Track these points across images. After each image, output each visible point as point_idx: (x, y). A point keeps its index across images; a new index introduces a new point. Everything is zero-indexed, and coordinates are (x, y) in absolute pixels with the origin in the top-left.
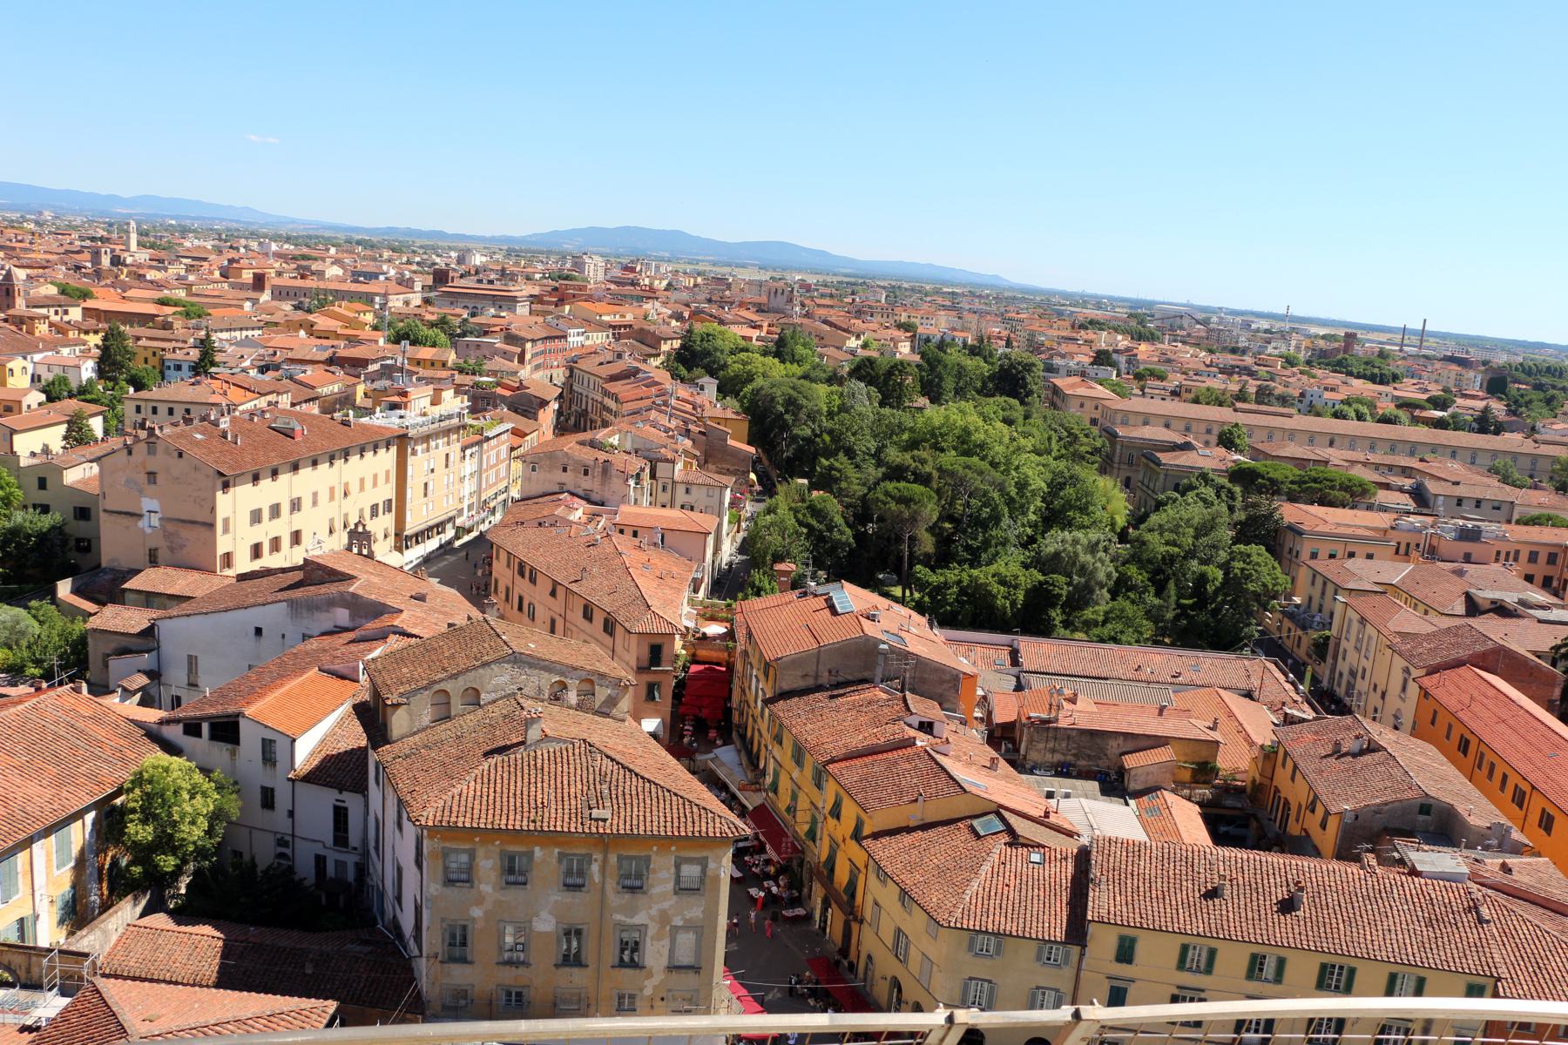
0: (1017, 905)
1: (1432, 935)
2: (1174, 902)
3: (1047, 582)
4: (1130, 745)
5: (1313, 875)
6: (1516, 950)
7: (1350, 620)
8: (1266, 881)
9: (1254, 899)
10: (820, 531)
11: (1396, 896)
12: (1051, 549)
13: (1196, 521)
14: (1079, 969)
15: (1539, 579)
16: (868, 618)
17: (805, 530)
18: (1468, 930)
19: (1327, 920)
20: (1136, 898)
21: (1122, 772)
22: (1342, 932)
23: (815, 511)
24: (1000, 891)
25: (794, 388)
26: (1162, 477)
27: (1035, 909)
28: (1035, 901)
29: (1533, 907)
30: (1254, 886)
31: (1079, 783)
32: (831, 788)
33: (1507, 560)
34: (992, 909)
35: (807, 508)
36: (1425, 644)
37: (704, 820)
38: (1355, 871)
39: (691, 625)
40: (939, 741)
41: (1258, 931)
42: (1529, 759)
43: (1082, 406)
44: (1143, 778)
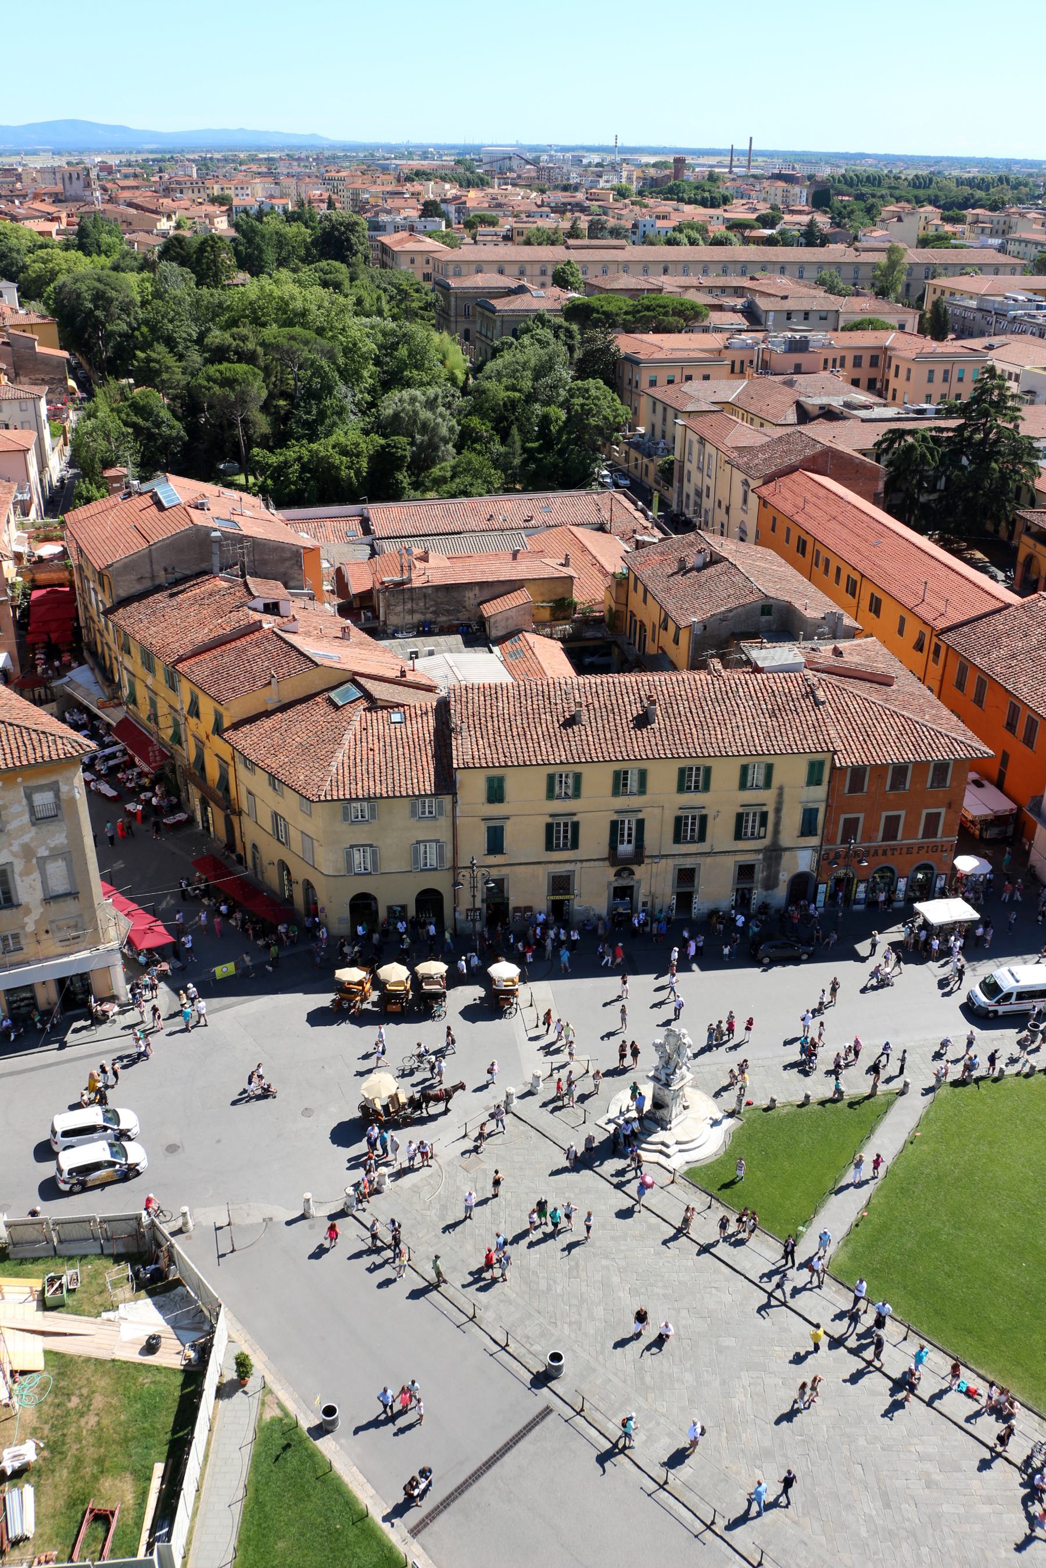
0: (383, 768)
2: (535, 737)
3: (389, 445)
4: (486, 594)
5: (664, 688)
6: (848, 723)
7: (691, 442)
8: (620, 701)
9: (611, 720)
10: (148, 429)
11: (742, 694)
12: (390, 412)
13: (533, 362)
14: (454, 817)
15: (864, 382)
16: (196, 508)
17: (130, 430)
18: (807, 713)
19: (680, 728)
20: (498, 738)
21: (482, 621)
22: (695, 736)
23: (138, 409)
24: (365, 757)
25: (99, 280)
26: (498, 324)
27: (402, 768)
28: (401, 760)
30: (610, 707)
31: (441, 639)
32: (185, 687)
33: (834, 367)
34: (359, 776)
35: (130, 406)
36: (760, 455)
37: (45, 745)
38: (703, 677)
39: (24, 549)
40: (286, 620)
41: (618, 749)
42: (858, 551)
43: (412, 261)
44: (503, 624)
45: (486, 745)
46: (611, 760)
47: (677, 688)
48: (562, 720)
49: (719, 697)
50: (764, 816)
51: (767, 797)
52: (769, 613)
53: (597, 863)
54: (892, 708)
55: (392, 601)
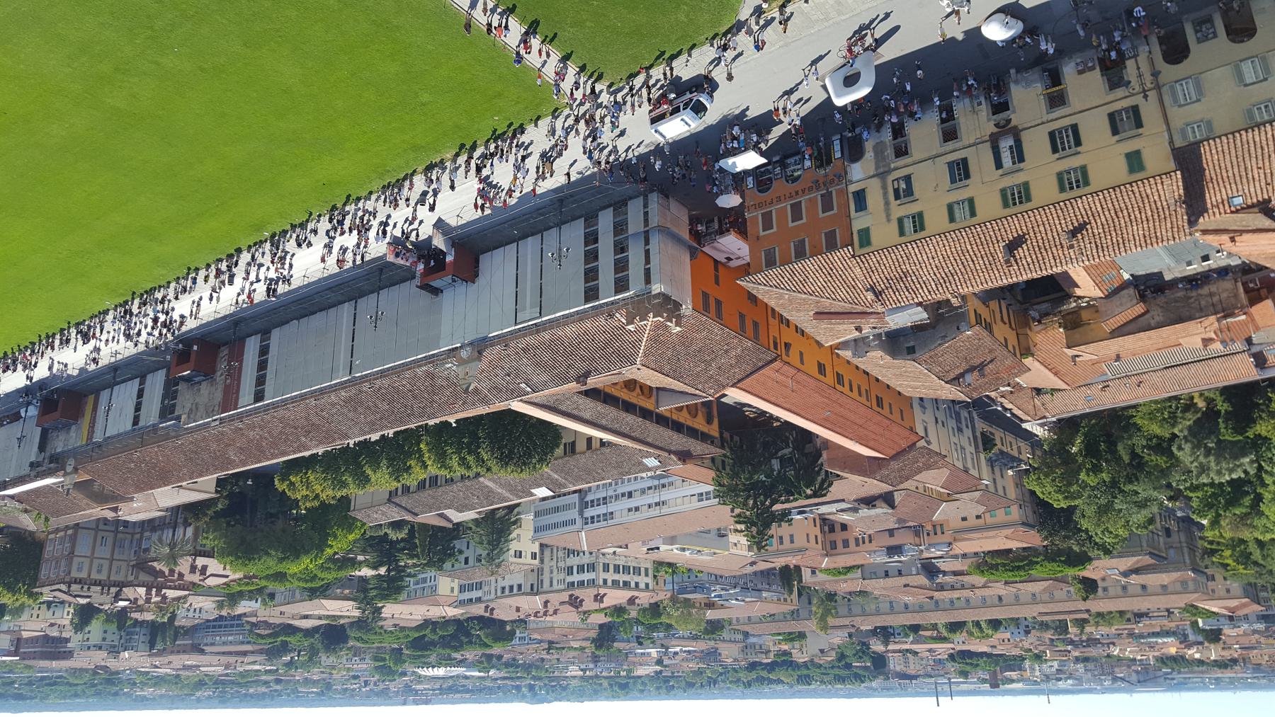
0: (1247, 155)
1: (903, 267)
2: (1107, 213)
5: (997, 275)
6: (846, 279)
7: (974, 468)
8: (1034, 257)
11: (933, 283)
15: (838, 528)
18: (879, 280)
19: (980, 247)
21: (1142, 298)
26: (1144, 544)
29: (841, 310)
30: (1043, 250)
33: (863, 538)
36: (921, 465)
41: (1033, 219)
42: (841, 406)
43: (1228, 591)
45: (1151, 196)
46: (1037, 209)
47: (987, 277)
48: (1084, 232)
49: (951, 278)
50: (897, 197)
51: (899, 211)
52: (908, 348)
53: (1029, 125)
54: (814, 298)
55: (1233, 300)
